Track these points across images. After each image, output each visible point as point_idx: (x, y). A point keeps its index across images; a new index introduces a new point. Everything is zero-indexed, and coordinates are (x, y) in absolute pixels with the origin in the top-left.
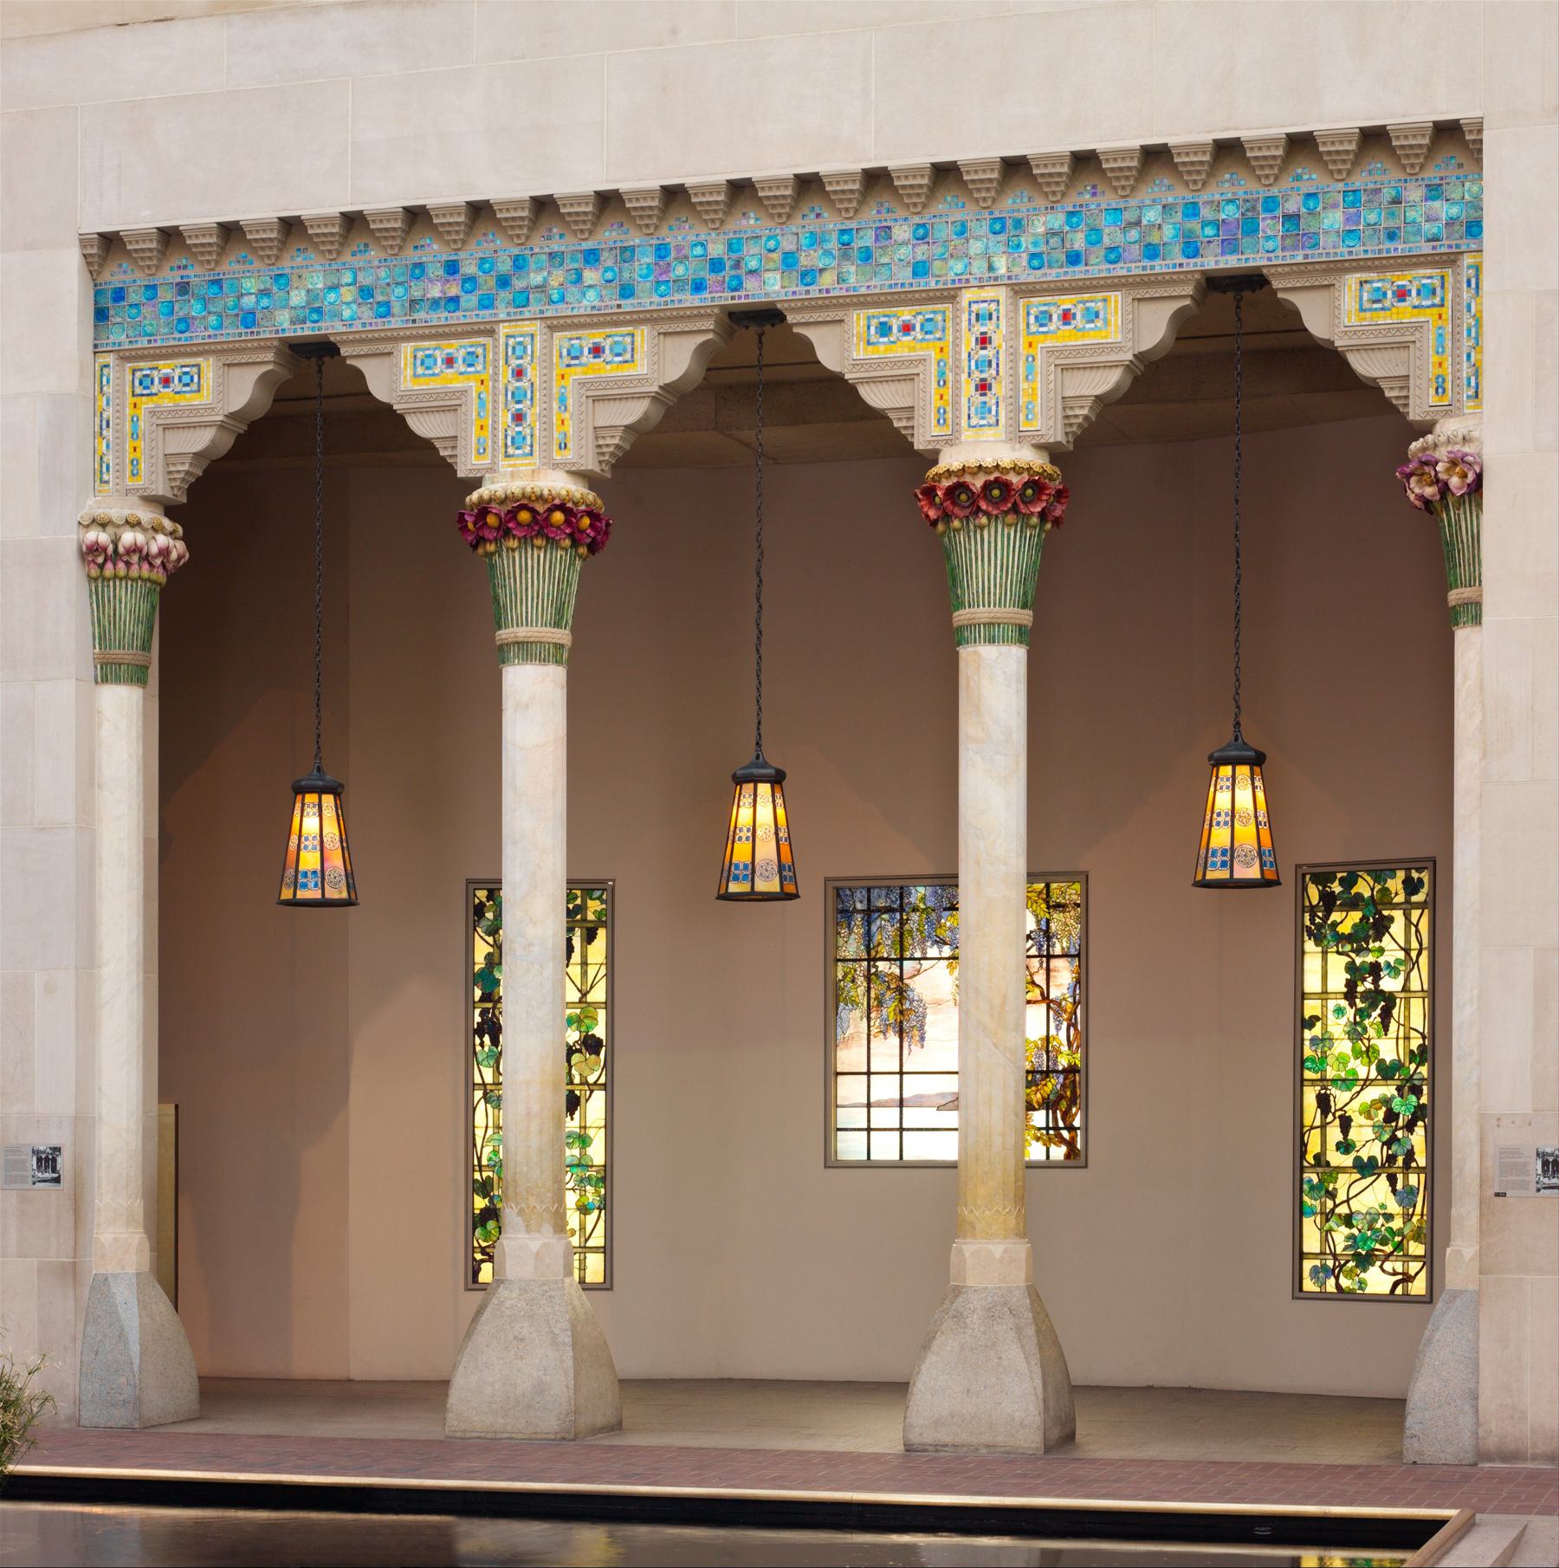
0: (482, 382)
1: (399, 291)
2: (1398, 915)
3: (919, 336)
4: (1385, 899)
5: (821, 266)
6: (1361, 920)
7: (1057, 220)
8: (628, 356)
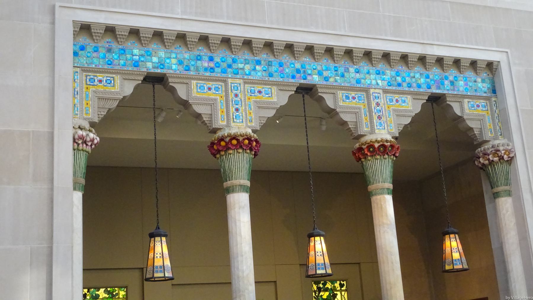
0: (221, 97)
1: (193, 63)
2: (339, 293)
3: (358, 101)
4: (334, 289)
5: (330, 76)
6: (329, 294)
7: (393, 73)
8: (270, 95)
